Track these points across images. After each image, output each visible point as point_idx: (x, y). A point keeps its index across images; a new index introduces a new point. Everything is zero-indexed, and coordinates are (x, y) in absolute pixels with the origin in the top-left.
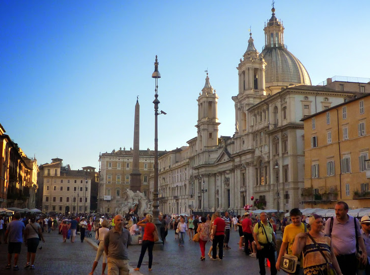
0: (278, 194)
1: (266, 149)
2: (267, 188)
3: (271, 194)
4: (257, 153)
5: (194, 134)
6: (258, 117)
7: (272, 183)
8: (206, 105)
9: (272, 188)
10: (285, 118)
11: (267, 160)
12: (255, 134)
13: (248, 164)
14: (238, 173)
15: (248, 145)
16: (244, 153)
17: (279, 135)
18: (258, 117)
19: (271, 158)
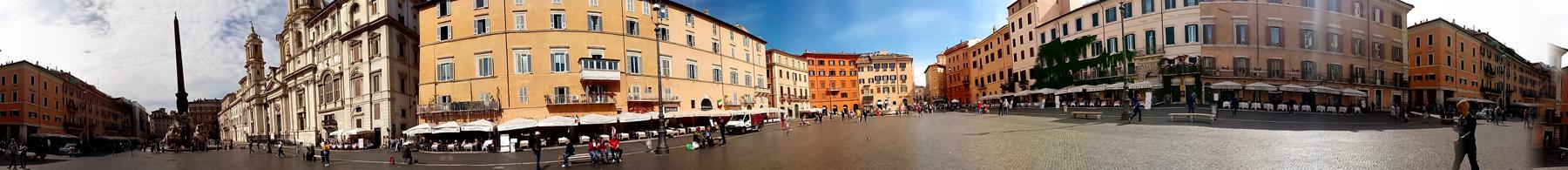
0: (359, 109)
1: (337, 59)
2: (339, 104)
3: (347, 110)
4: (321, 67)
5: (243, 73)
6: (322, 28)
7: (347, 95)
8: (252, 49)
9: (347, 102)
10: (374, 11)
11: (337, 70)
12: (315, 49)
13: (307, 83)
14: (293, 96)
15: (305, 60)
16: (302, 73)
17: (364, 37)
18: (322, 28)
19: (346, 65)
